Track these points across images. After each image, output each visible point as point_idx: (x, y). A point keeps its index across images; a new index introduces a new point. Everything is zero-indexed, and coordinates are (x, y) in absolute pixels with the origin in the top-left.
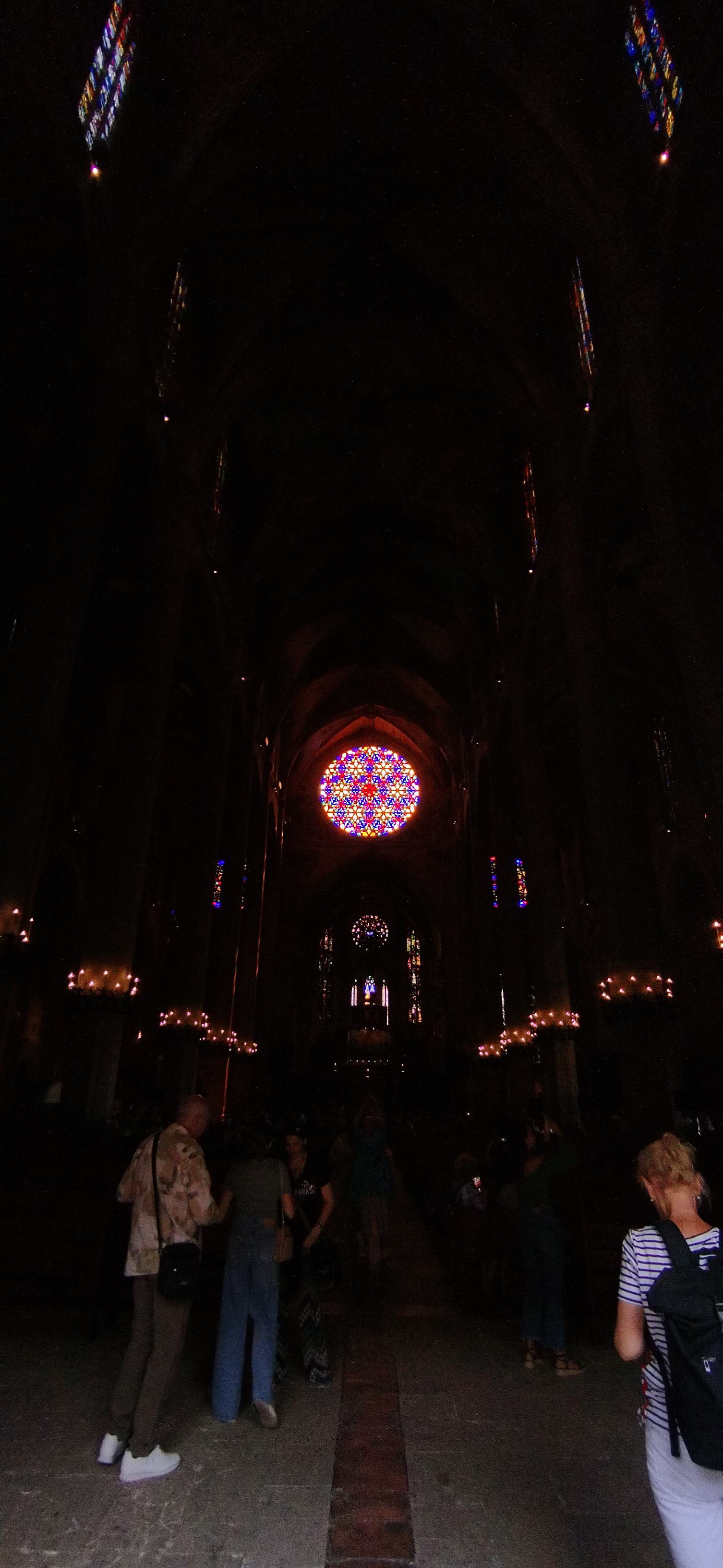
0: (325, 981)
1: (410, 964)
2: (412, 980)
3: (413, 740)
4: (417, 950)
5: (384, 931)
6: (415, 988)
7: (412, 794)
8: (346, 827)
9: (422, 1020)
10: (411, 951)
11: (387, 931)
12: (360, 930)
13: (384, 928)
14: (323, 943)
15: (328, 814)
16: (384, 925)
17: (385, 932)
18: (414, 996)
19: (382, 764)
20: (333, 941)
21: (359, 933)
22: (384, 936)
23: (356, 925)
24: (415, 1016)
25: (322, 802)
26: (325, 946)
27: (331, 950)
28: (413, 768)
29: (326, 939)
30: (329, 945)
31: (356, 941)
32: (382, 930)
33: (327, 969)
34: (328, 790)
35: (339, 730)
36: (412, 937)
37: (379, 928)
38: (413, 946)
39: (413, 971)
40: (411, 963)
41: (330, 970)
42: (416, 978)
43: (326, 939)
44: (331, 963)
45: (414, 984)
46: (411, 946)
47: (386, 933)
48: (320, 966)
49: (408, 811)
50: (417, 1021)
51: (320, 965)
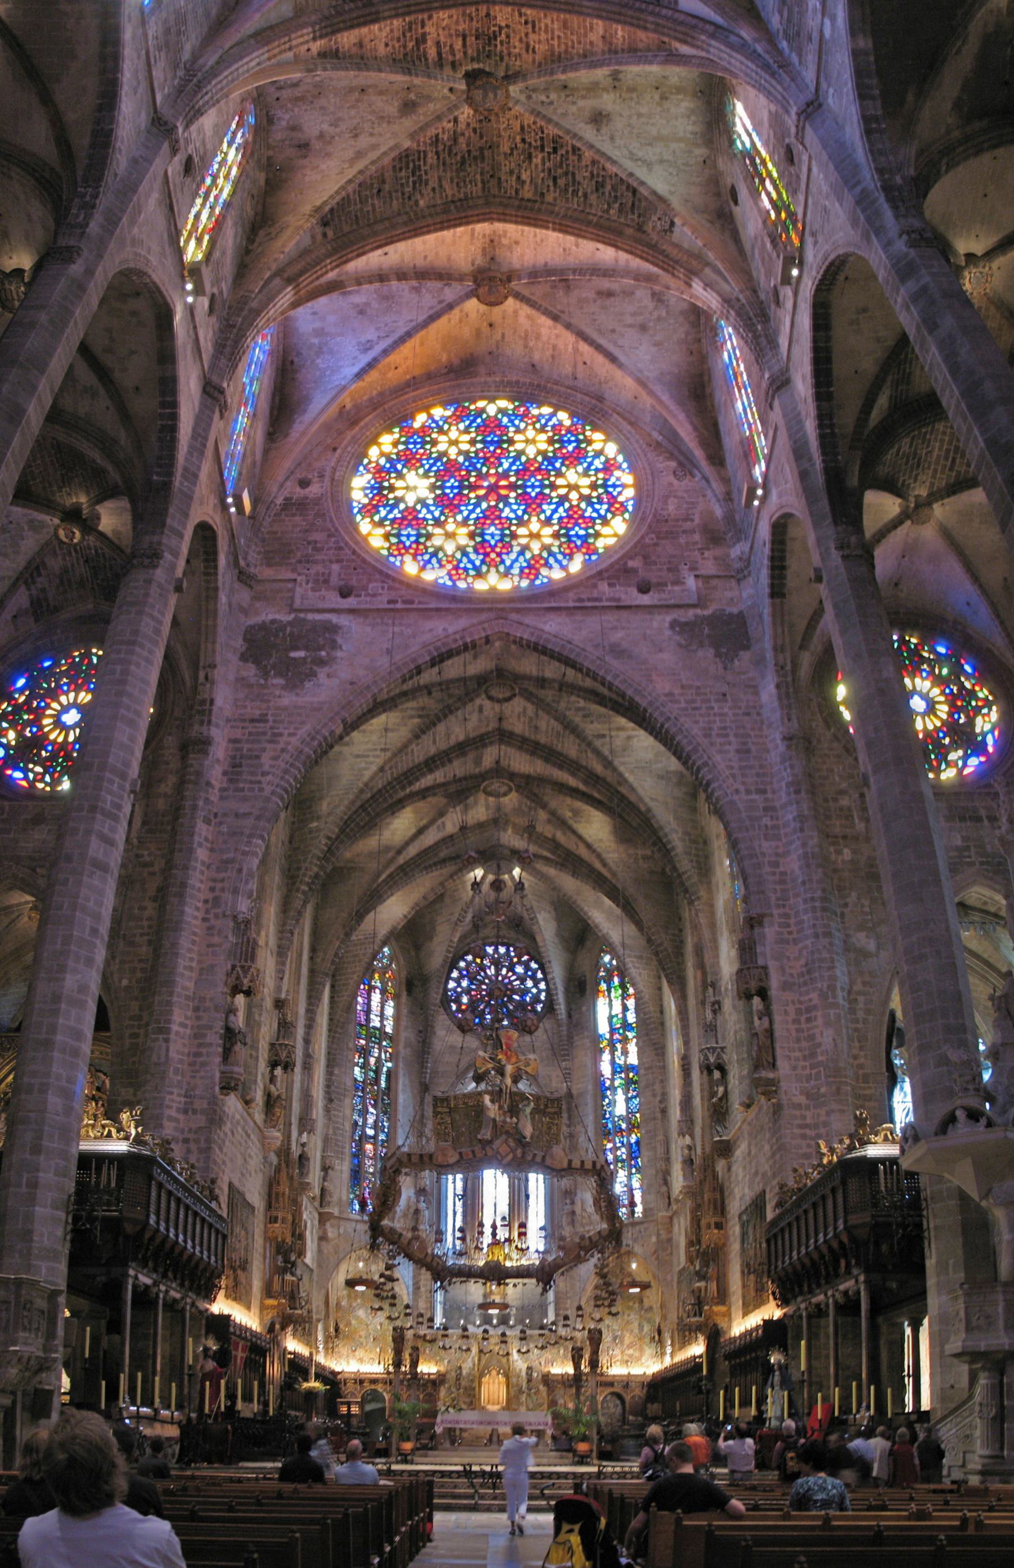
0: (371, 1110)
4: (626, 1026)
5: (536, 985)
10: (613, 1030)
11: (542, 986)
13: (533, 978)
14: (368, 1012)
16: (535, 972)
21: (468, 991)
23: (460, 971)
26: (372, 1017)
27: (389, 1029)
29: (376, 997)
30: (382, 1016)
32: (529, 983)
33: (377, 1081)
35: (409, 335)
40: (613, 1062)
41: (388, 1080)
43: (376, 997)
44: (389, 1065)
46: (611, 1018)
47: (540, 991)
51: (357, 1064)
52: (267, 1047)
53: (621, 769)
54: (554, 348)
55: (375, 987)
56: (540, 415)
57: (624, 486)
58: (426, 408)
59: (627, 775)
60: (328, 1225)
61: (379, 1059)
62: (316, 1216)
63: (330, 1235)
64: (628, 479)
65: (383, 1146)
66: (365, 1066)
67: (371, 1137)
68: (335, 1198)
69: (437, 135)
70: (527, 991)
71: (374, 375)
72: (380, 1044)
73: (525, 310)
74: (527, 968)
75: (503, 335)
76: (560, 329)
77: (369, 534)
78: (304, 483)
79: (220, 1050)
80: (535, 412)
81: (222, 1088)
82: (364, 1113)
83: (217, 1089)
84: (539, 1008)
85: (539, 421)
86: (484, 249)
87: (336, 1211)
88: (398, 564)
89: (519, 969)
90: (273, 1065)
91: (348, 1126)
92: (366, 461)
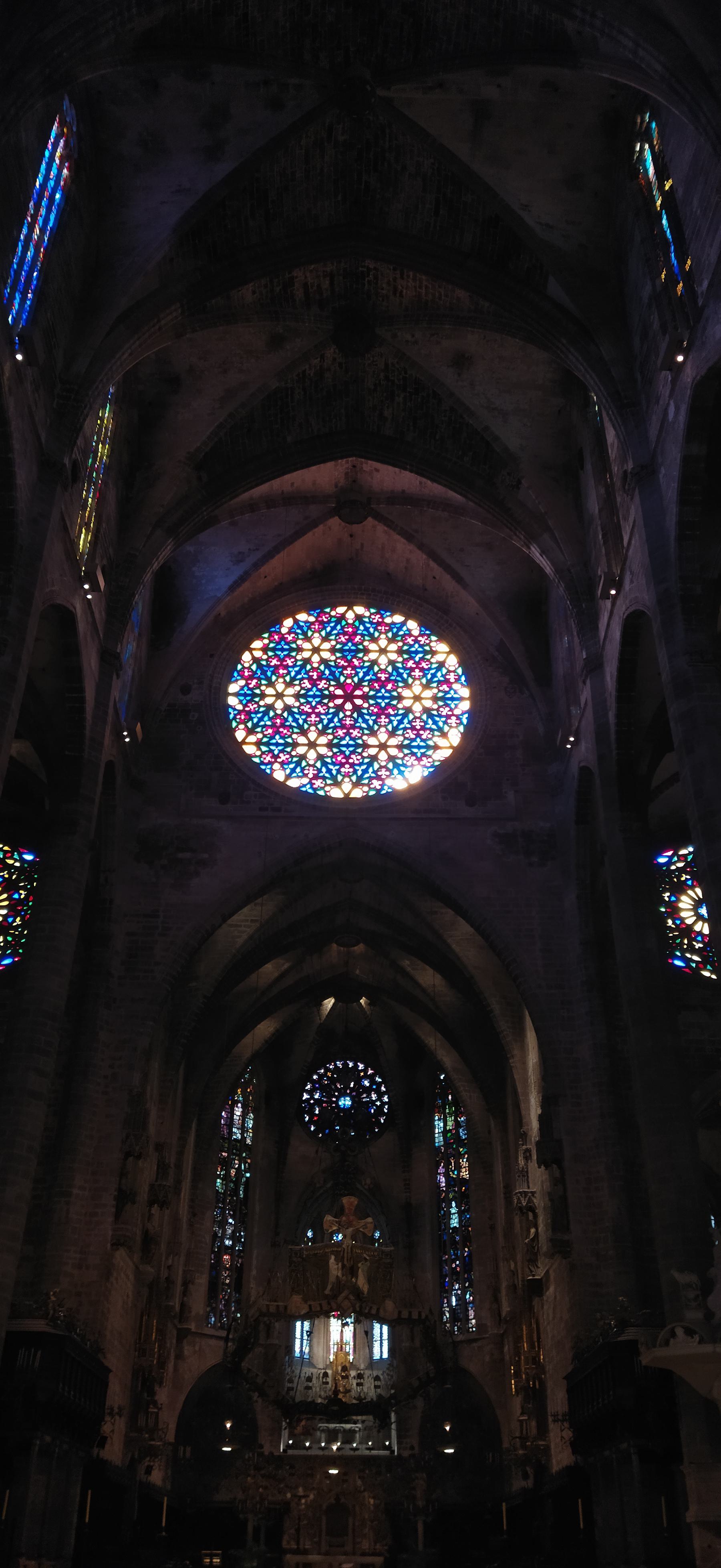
0: (230, 1221)
1: (443, 1179)
2: (450, 1219)
3: (458, 579)
5: (380, 1098)
6: (458, 1238)
7: (453, 706)
8: (288, 777)
9: (477, 1325)
11: (386, 1099)
12: (321, 1096)
14: (230, 1123)
15: (245, 747)
17: (381, 1101)
18: (454, 1261)
19: (380, 642)
20: (253, 1120)
21: (318, 1102)
22: (380, 1109)
23: (313, 1082)
24: (459, 1315)
25: (235, 730)
26: (234, 1130)
27: (248, 1141)
28: (454, 649)
29: (238, 1111)
31: (311, 1122)
32: (374, 1097)
33: (236, 1192)
34: (249, 696)
35: (276, 550)
36: (447, 1111)
37: (368, 1091)
38: (450, 1131)
39: (451, 1196)
40: (447, 1175)
42: (460, 1213)
43: (238, 1111)
44: (248, 1175)
45: (455, 1227)
46: (445, 1132)
47: (383, 1104)
48: (218, 1180)
49: (441, 742)
50: (464, 1329)
51: (219, 1177)
52: (146, 1188)
53: (449, 941)
54: (408, 560)
55: (238, 1102)
56: (393, 623)
57: (461, 699)
58: (292, 614)
59: (454, 946)
60: (185, 1341)
61: (239, 1170)
62: (175, 1332)
63: (186, 1353)
64: (465, 692)
65: (239, 1256)
66: (226, 1178)
67: (227, 1247)
68: (193, 1313)
69: (304, 371)
70: (373, 1103)
71: (246, 585)
72: (240, 1155)
73: (381, 528)
74: (373, 1082)
75: (362, 545)
76: (411, 547)
77: (244, 742)
78: (186, 690)
79: (113, 1210)
80: (388, 620)
81: (112, 1245)
82: (223, 1224)
83: (109, 1245)
84: (382, 1121)
85: (391, 629)
86: (347, 474)
87: (193, 1327)
88: (268, 771)
89: (366, 1083)
90: (151, 1204)
91: (208, 1239)
92: (239, 667)
